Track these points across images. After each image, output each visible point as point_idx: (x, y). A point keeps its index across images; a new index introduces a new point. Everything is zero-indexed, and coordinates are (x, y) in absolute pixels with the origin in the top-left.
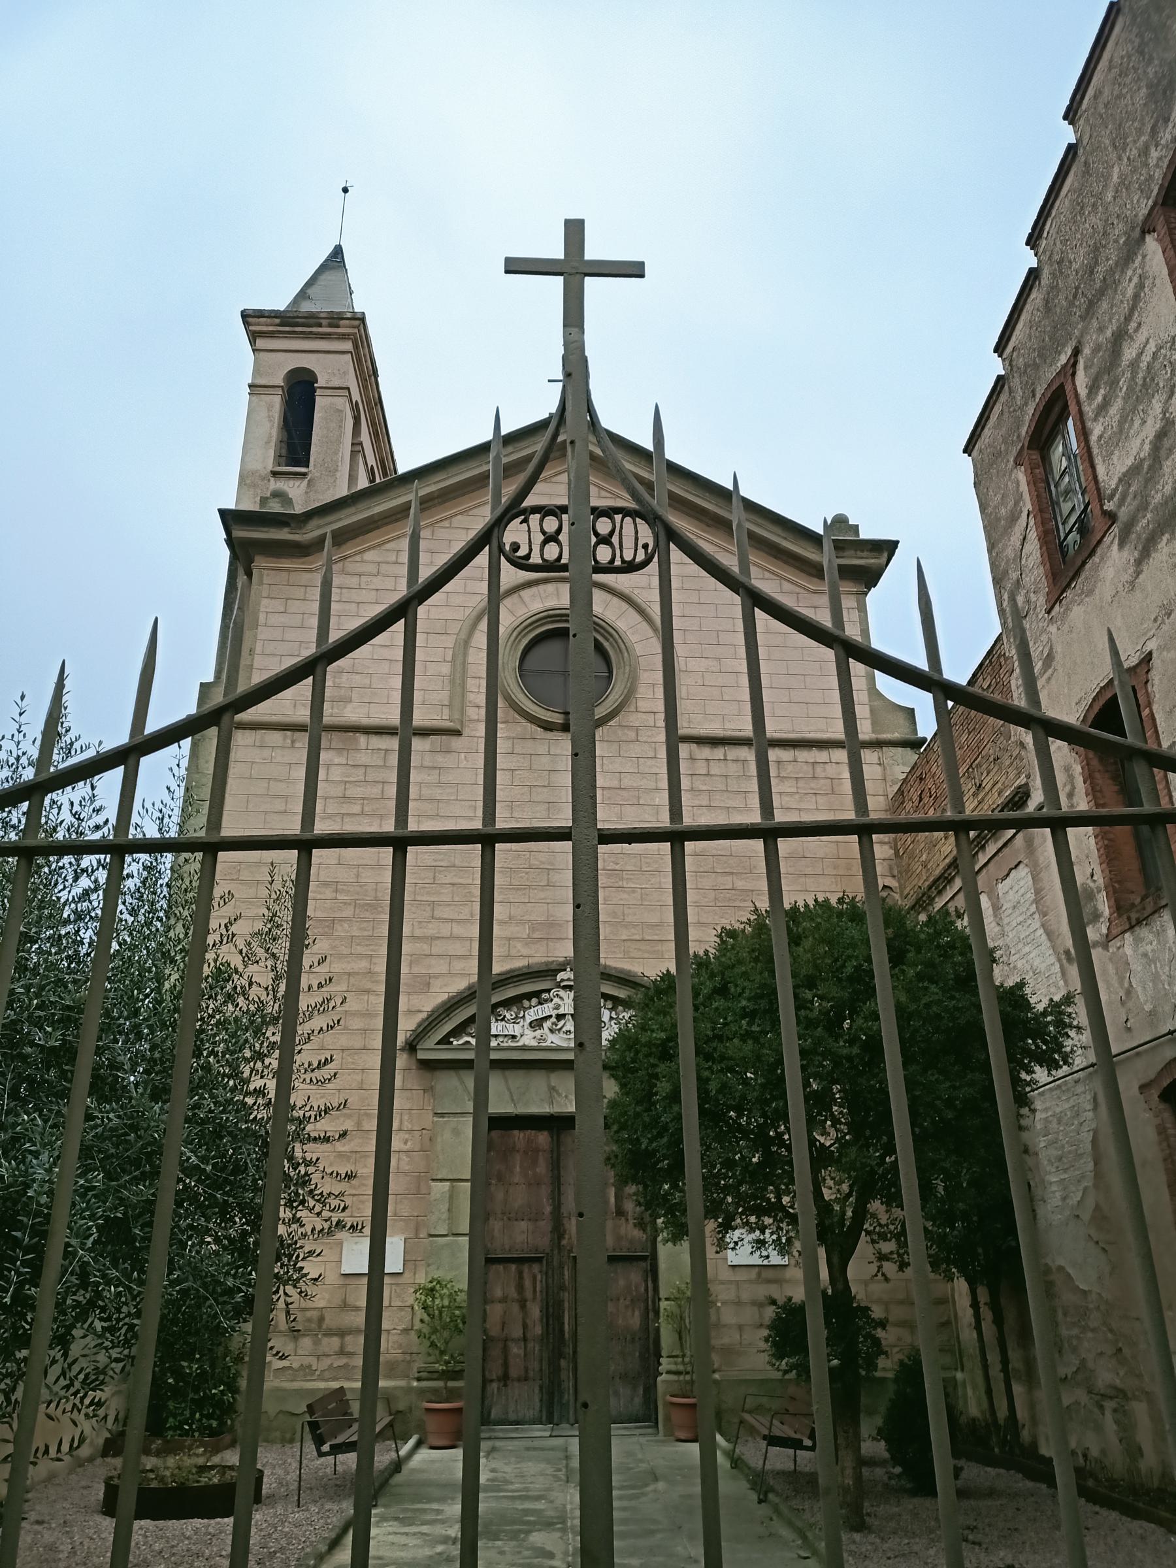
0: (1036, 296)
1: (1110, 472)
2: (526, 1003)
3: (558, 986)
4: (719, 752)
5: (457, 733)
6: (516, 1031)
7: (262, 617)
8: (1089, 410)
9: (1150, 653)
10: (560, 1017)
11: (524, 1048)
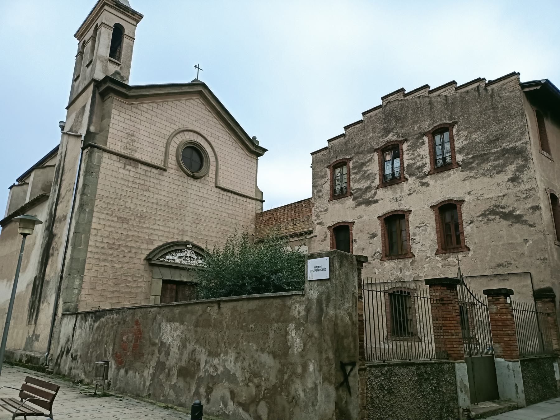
3: (187, 248)
4: (225, 193)
5: (165, 170)
6: (174, 258)
7: (112, 115)
10: (187, 257)
11: (177, 263)
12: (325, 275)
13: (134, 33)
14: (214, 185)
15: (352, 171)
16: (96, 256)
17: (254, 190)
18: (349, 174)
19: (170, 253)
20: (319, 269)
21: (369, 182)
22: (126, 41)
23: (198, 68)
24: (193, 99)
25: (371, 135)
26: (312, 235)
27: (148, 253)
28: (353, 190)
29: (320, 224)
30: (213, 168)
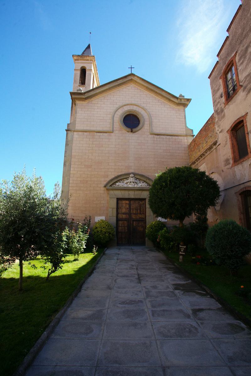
0: (228, 43)
1: (242, 77)
2: (125, 180)
4: (159, 137)
8: (238, 64)
9: (248, 113)
10: (130, 182)
14: (149, 134)
16: (74, 188)
17: (185, 130)
24: (127, 86)
26: (218, 144)
27: (105, 183)
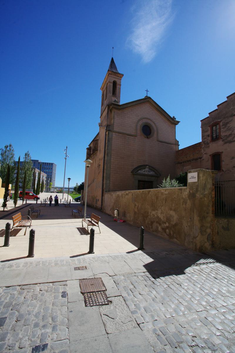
4: (161, 143)
5: (136, 136)
12: (196, 180)
13: (121, 83)
15: (222, 127)
17: (174, 141)
18: (220, 129)
19: (140, 170)
20: (193, 177)
21: (231, 132)
22: (118, 86)
23: (147, 91)
25: (232, 108)
26: (202, 159)
28: (222, 137)
29: (205, 154)
30: (156, 133)
